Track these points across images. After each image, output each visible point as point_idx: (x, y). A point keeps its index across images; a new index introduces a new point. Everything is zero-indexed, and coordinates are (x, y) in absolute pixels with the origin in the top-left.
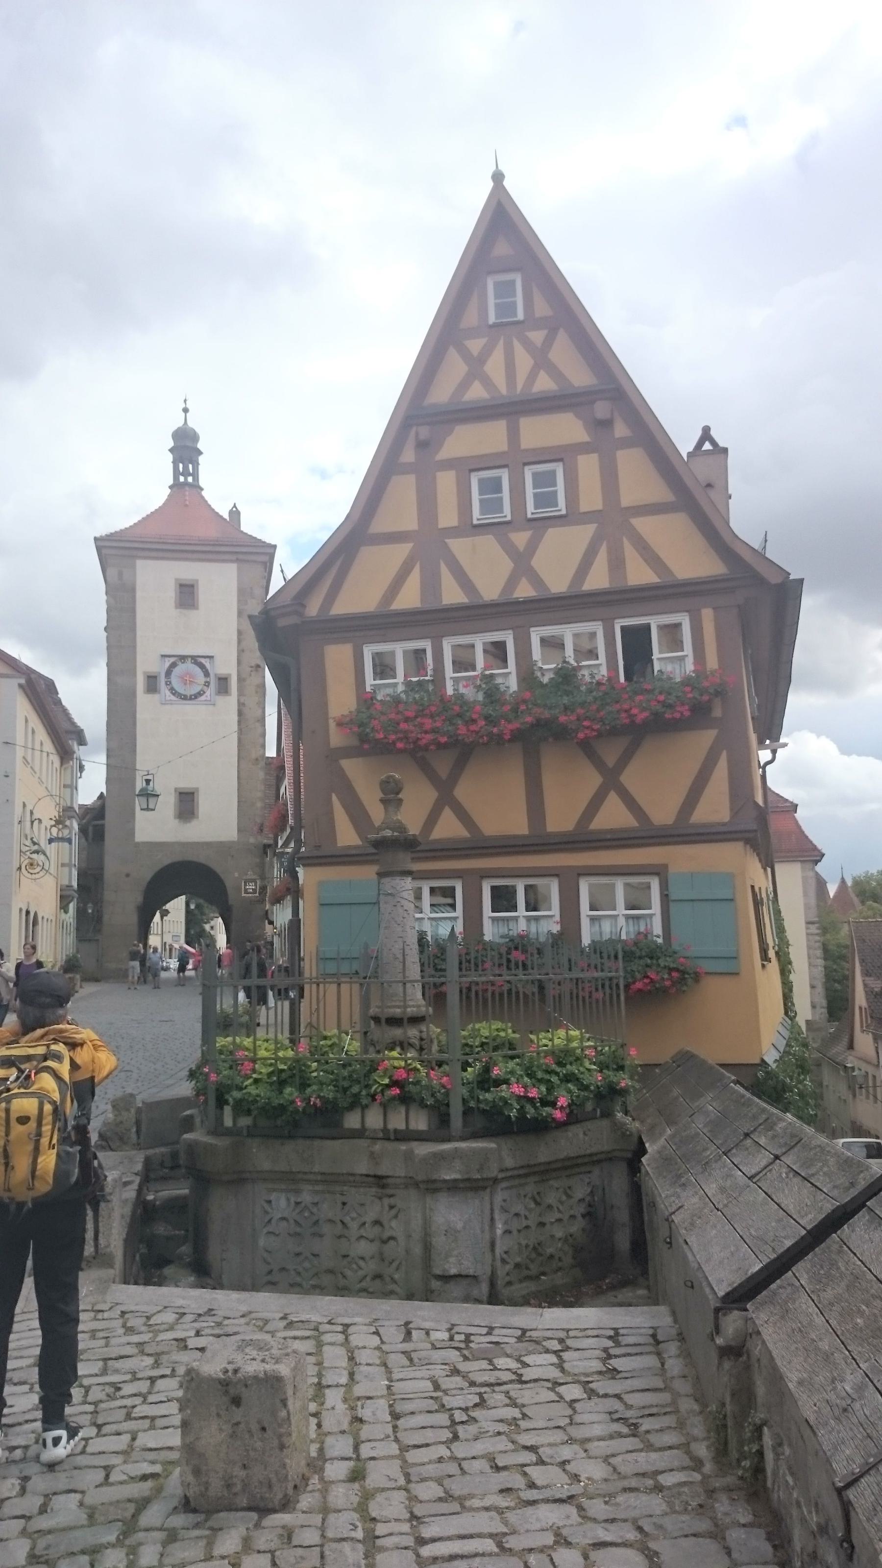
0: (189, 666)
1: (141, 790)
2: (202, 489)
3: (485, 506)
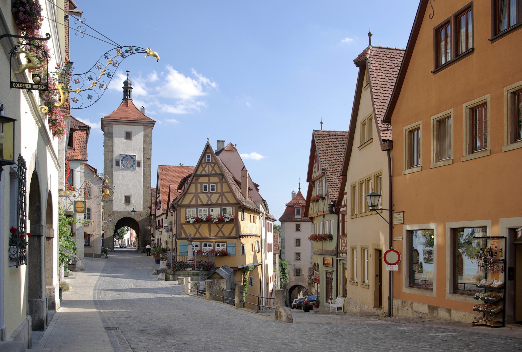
1: (132, 210)
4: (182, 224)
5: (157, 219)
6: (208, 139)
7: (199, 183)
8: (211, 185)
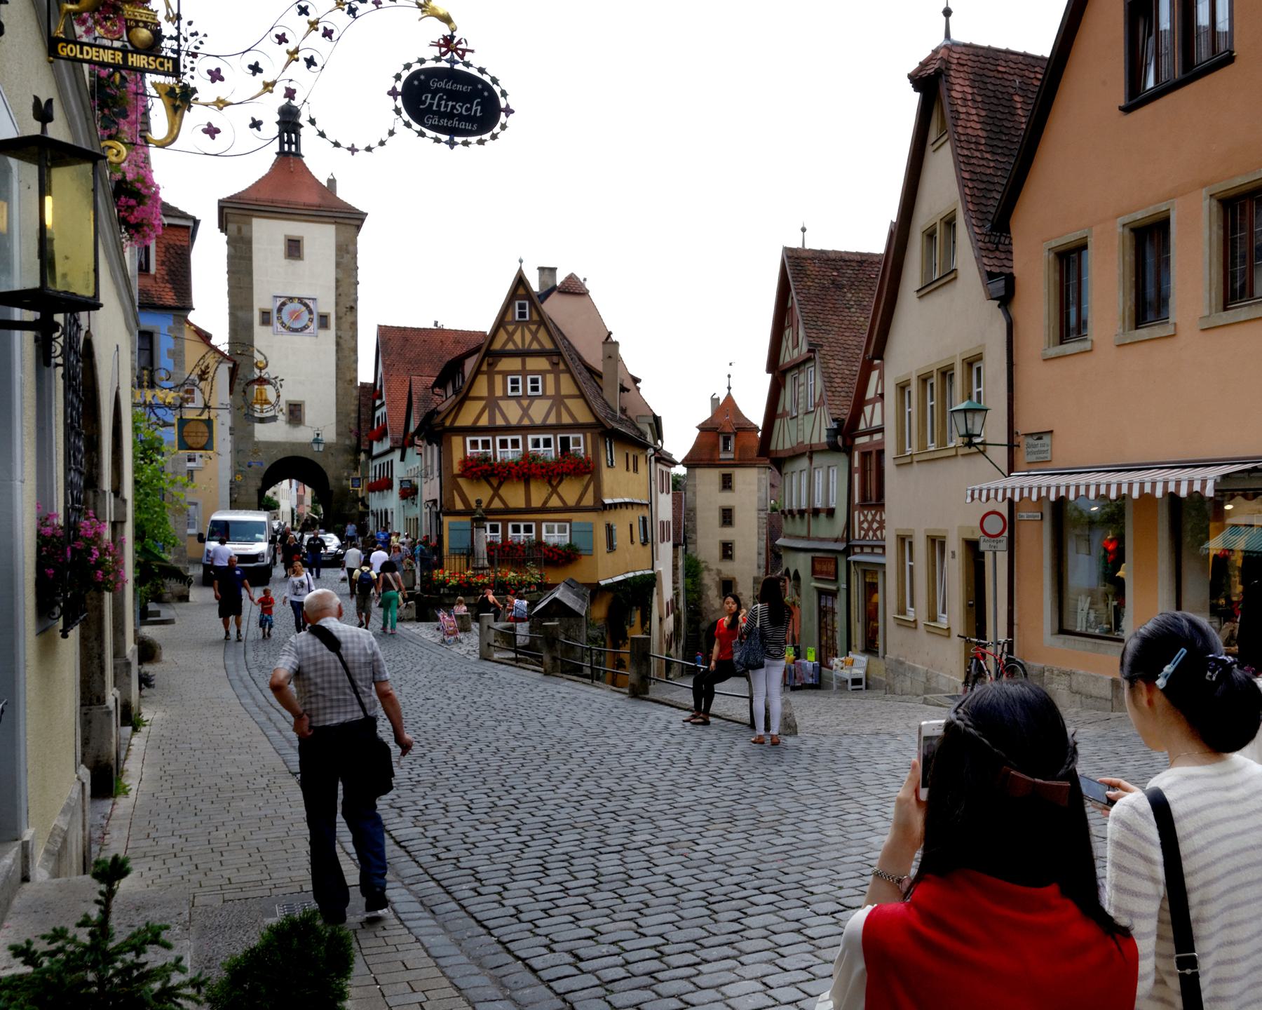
0: (295, 305)
3: (513, 389)
5: (377, 462)
6: (521, 261)
7: (499, 372)
8: (529, 378)
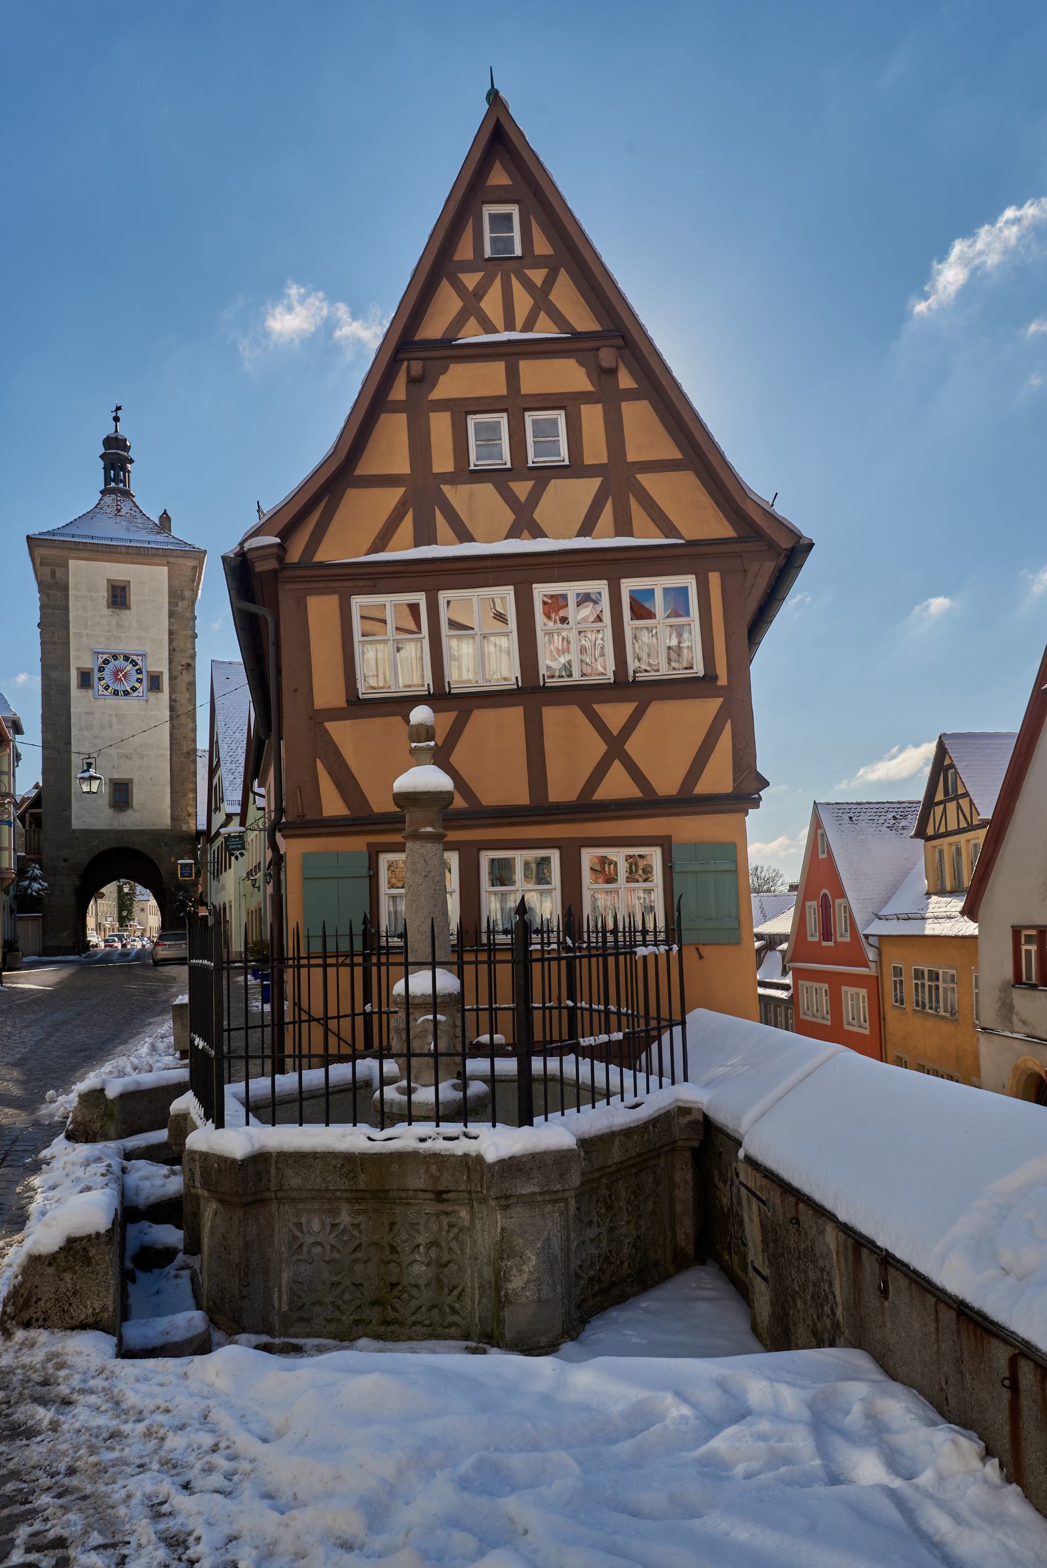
0: (121, 662)
2: (134, 497)
4: (318, 718)
8: (529, 417)
